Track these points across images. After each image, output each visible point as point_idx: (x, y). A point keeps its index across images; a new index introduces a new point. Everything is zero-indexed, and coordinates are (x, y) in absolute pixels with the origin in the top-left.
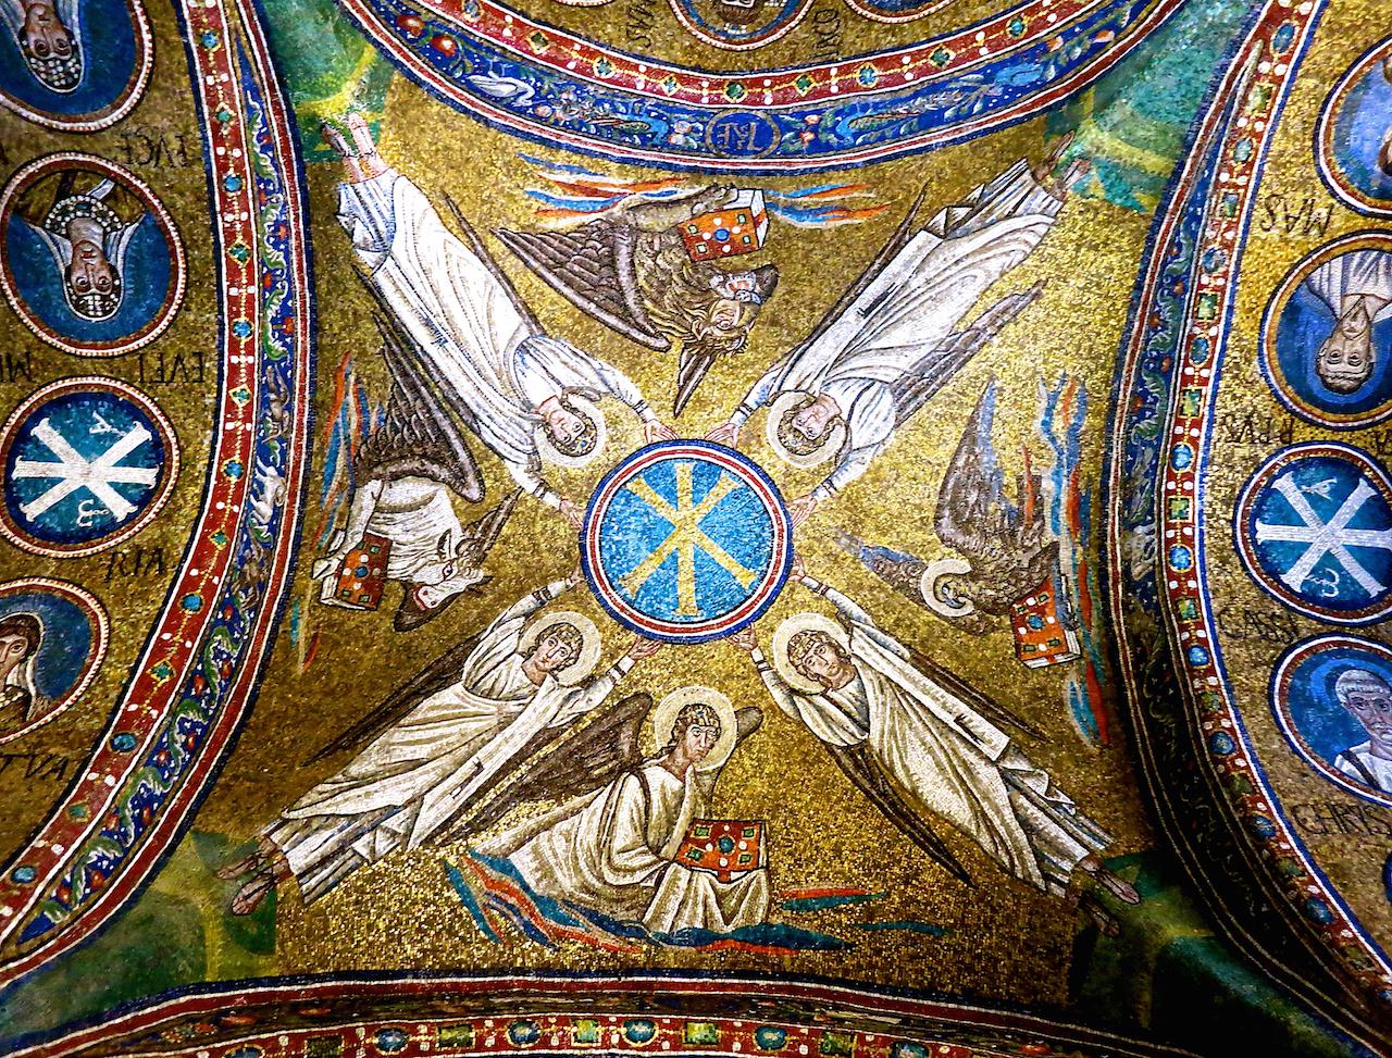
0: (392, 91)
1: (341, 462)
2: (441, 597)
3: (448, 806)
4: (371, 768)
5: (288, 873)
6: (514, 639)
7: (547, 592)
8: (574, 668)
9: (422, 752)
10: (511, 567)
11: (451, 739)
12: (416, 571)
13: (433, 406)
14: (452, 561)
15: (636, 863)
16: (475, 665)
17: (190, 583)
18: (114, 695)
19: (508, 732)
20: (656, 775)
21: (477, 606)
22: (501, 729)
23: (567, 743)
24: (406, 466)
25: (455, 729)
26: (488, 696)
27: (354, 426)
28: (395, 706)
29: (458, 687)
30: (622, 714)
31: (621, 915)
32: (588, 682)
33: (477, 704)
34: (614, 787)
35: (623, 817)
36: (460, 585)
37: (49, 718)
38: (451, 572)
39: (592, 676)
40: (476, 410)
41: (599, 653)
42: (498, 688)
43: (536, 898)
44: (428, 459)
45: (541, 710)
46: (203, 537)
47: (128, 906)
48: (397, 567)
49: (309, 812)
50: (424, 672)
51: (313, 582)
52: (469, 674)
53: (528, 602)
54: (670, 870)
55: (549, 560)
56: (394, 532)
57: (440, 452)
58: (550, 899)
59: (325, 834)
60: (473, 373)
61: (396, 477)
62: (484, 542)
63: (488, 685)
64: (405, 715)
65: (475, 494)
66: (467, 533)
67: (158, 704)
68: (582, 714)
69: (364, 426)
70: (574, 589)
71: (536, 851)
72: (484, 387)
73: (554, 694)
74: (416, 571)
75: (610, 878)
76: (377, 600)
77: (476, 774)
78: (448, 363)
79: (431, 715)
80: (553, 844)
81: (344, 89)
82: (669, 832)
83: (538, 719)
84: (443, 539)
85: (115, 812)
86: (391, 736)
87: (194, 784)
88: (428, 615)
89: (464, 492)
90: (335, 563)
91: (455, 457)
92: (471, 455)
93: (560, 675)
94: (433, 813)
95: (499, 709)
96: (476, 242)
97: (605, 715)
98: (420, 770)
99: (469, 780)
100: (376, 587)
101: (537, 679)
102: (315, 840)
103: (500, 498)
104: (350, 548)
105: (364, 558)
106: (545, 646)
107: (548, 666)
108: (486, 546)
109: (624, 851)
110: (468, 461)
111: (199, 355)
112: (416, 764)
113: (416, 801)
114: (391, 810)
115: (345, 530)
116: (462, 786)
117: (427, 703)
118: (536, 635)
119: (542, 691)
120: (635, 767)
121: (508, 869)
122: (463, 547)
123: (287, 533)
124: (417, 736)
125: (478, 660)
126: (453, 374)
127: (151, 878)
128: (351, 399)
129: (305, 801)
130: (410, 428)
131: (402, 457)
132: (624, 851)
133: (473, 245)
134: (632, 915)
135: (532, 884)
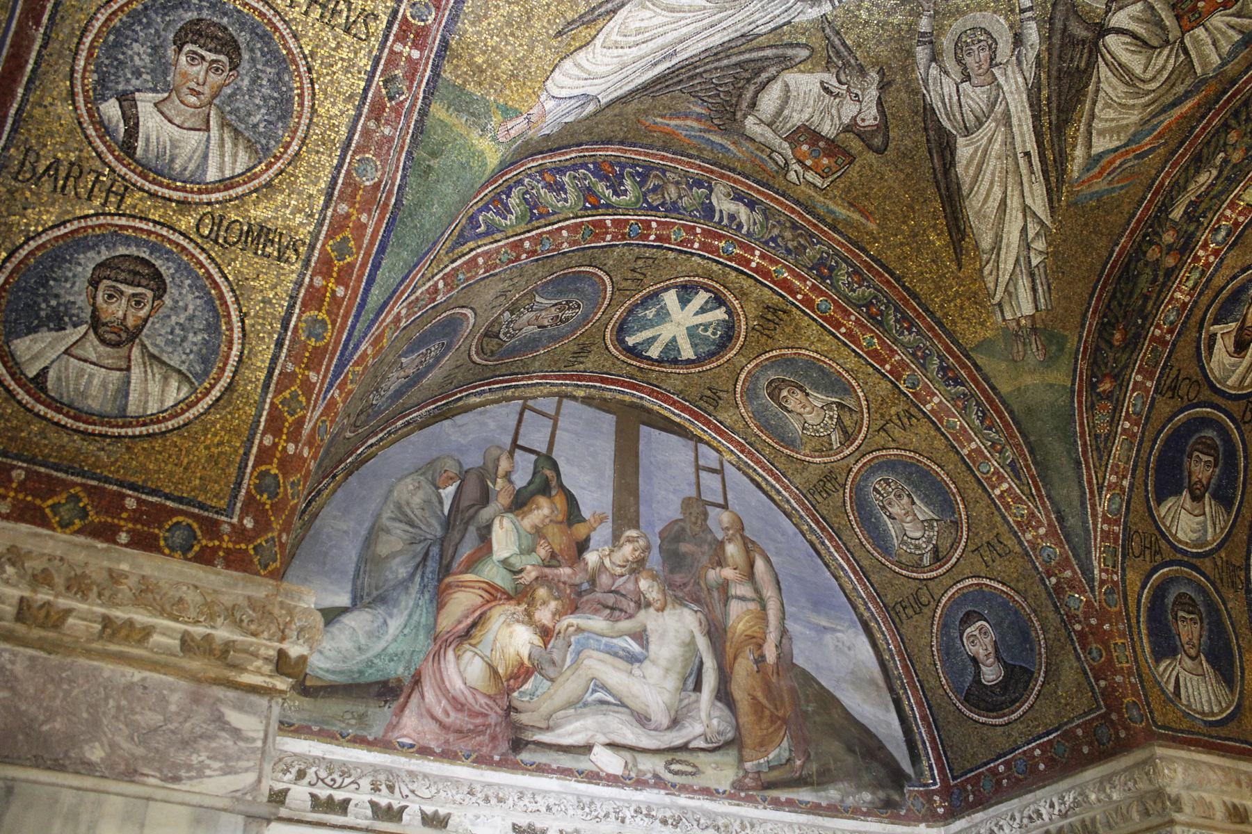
0: (464, 82)
1: (716, 139)
2: (874, 111)
3: (1040, 190)
4: (991, 234)
5: (1033, 316)
6: (945, 79)
7: (923, 34)
8: (1001, 45)
9: (997, 193)
10: (883, 51)
11: (998, 169)
12: (840, 118)
13: (716, 64)
14: (848, 90)
15: (1161, 61)
16: (949, 119)
17: (808, 302)
18: (871, 370)
19: (1015, 121)
20: (1120, 19)
21: (898, 91)
22: (1011, 126)
23: (1049, 77)
24: (748, 95)
25: (992, 162)
26: (981, 124)
27: (695, 124)
28: (948, 189)
29: (961, 141)
30: (1059, 25)
31: (1180, 89)
32: (1018, 40)
33: (982, 135)
34: (1102, 56)
35: (1125, 57)
36: (873, 93)
37: (863, 403)
38: (857, 95)
39: (1016, 34)
40: (738, 34)
41: (1002, 20)
42: (979, 112)
43: (1126, 145)
44: (752, 78)
45: (1014, 87)
46: (774, 283)
47: (1011, 413)
48: (827, 129)
49: (1001, 289)
50: (931, 155)
51: (802, 187)
52: (954, 127)
53: (922, 53)
54: (1187, 40)
55: (897, 19)
56: (797, 119)
57: (757, 67)
58: (1134, 135)
59: (1020, 282)
60: (711, 31)
61: (753, 105)
62: (848, 61)
63: (972, 117)
64: (959, 188)
65: (804, 53)
66: (834, 70)
67: (893, 352)
68: (1038, 55)
69: (699, 117)
70: (936, 12)
71: (1101, 133)
72: (724, 24)
73: (1009, 72)
74: (840, 118)
75: (1154, 85)
76: (846, 153)
77: (1030, 162)
78: (694, 48)
79: (971, 171)
80: (1106, 116)
81: (480, 148)
82: (1164, 28)
83: (1020, 94)
84: (826, 89)
85: (954, 399)
86: (972, 207)
87: (931, 329)
88: (884, 124)
89: (797, 60)
90: (796, 167)
91: (767, 58)
92: (771, 46)
93: (998, 60)
94: (1039, 201)
95: (995, 120)
96: (603, 10)
97: (1050, 38)
98: (1009, 202)
99: (1031, 165)
100: (833, 148)
101: (989, 80)
102: (1021, 290)
103: (820, 34)
104: (790, 152)
105: (805, 147)
106: (969, 60)
107: (985, 66)
108: (852, 61)
109: (1146, 68)
110: (774, 51)
111: (638, 258)
112: (1003, 202)
113: (1025, 209)
114: (1024, 230)
115: (773, 151)
116: (1032, 172)
117: (960, 169)
118: (954, 62)
119: (1001, 80)
120: (1102, 30)
121: (1100, 156)
122: (843, 78)
123: (750, 187)
124: (983, 191)
125: (947, 114)
126: (701, 46)
127: (993, 388)
128: (673, 123)
129: (991, 285)
130: (721, 85)
131: (740, 96)
132: (1146, 68)
133: (607, 13)
134: (1188, 81)
135: (1117, 143)
